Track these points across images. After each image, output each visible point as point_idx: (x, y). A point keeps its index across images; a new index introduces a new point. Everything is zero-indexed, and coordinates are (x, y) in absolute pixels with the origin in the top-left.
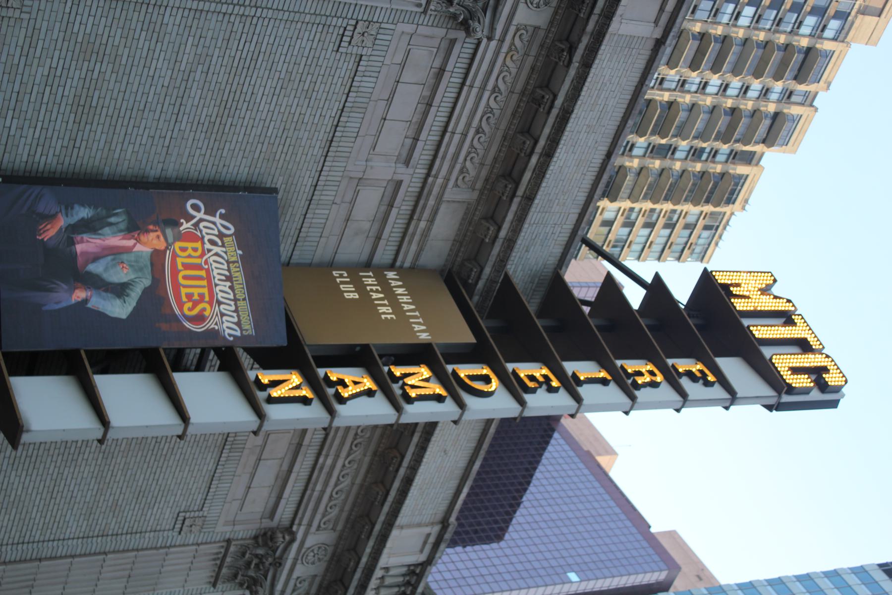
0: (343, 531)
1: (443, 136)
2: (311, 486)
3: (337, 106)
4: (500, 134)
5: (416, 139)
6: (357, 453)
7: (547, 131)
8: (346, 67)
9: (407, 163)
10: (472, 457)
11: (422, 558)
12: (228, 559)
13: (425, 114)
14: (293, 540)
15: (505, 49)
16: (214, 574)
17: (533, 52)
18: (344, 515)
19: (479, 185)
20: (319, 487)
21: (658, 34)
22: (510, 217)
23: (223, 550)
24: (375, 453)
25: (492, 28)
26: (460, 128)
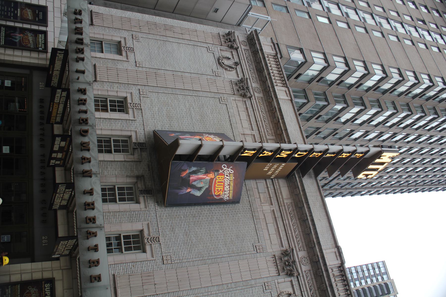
0: (307, 250)
1: (257, 123)
3: (228, 116)
4: (270, 122)
5: (251, 124)
7: (278, 114)
8: (224, 107)
9: (253, 130)
11: (340, 262)
12: (278, 262)
13: (249, 118)
14: (293, 250)
15: (258, 102)
17: (264, 102)
18: (304, 243)
19: (274, 134)
20: (290, 232)
21: (290, 99)
22: (285, 136)
24: (299, 219)
25: (251, 94)
26: (260, 120)
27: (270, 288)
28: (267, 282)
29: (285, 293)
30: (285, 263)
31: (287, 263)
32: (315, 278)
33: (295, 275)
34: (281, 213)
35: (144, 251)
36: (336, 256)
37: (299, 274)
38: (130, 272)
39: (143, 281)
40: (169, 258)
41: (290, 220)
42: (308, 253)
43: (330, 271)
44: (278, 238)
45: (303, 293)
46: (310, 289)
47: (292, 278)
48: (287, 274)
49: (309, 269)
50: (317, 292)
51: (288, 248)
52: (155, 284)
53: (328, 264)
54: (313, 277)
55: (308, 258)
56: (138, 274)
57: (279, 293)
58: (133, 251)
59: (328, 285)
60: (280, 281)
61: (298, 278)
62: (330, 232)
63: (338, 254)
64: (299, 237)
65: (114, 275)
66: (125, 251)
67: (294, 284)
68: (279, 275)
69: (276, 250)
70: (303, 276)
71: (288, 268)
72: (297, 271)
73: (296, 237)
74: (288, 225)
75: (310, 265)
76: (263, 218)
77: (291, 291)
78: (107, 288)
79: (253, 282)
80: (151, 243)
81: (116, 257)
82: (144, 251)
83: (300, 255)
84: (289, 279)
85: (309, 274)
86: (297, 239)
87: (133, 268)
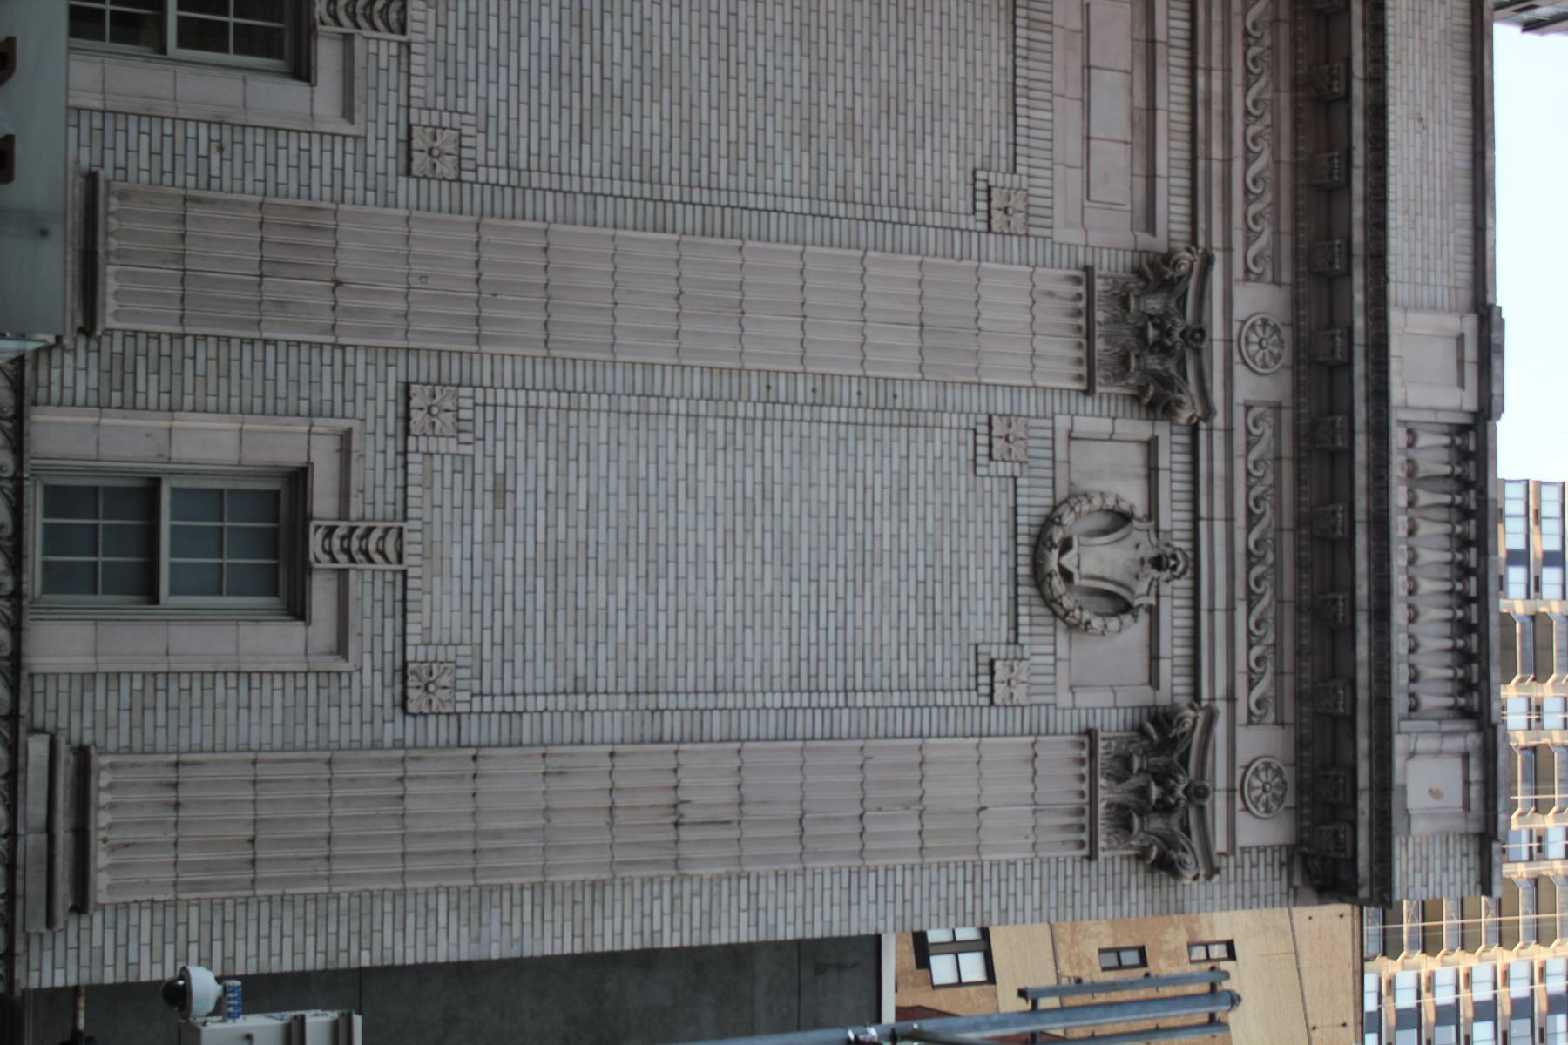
0: (1295, 285)
2: (1201, 147)
6: (1262, 82)
10: (1474, 144)
11: (1471, 404)
12: (1100, 316)
14: (1208, 261)
16: (1082, 354)
18: (1286, 241)
20: (1217, 152)
23: (1082, 289)
24: (1295, 85)
27: (1018, 451)
28: (1008, 417)
29: (1097, 502)
30: (1144, 329)
31: (1152, 333)
32: (1297, 460)
33: (1184, 416)
34: (1193, 20)
35: (302, 71)
36: (1461, 362)
37: (1209, 412)
38: (191, 180)
39: (270, 254)
40: (446, 141)
41: (1238, 77)
42: (1296, 303)
43: (1398, 437)
44: (1139, 169)
45: (1203, 525)
46: (1249, 512)
47: (1162, 430)
48: (1136, 399)
49: (1272, 397)
50: (1288, 540)
51: (1180, 245)
52: (338, 283)
53: (1396, 394)
54: (1287, 449)
55: (1286, 333)
56: (244, 205)
57: (1062, 493)
58: (230, 58)
59: (1360, 516)
60: (1084, 425)
61: (1194, 431)
62: (1463, 210)
63: (1471, 353)
64: (1268, 198)
65: (91, 178)
66: (182, 43)
67: (1163, 461)
68: (1089, 392)
69: (1111, 242)
70: (1229, 431)
71: (1153, 363)
72: (1204, 393)
73: (1247, 191)
74: (1216, 107)
75: (1286, 378)
76: (1077, 24)
77: (1133, 496)
78: (44, 233)
79: (924, 397)
80: (348, 28)
81: (128, 77)
82: (302, 71)
83: (1246, 301)
84: (1143, 429)
85: (1266, 430)
86: (1247, 203)
87: (215, 158)
